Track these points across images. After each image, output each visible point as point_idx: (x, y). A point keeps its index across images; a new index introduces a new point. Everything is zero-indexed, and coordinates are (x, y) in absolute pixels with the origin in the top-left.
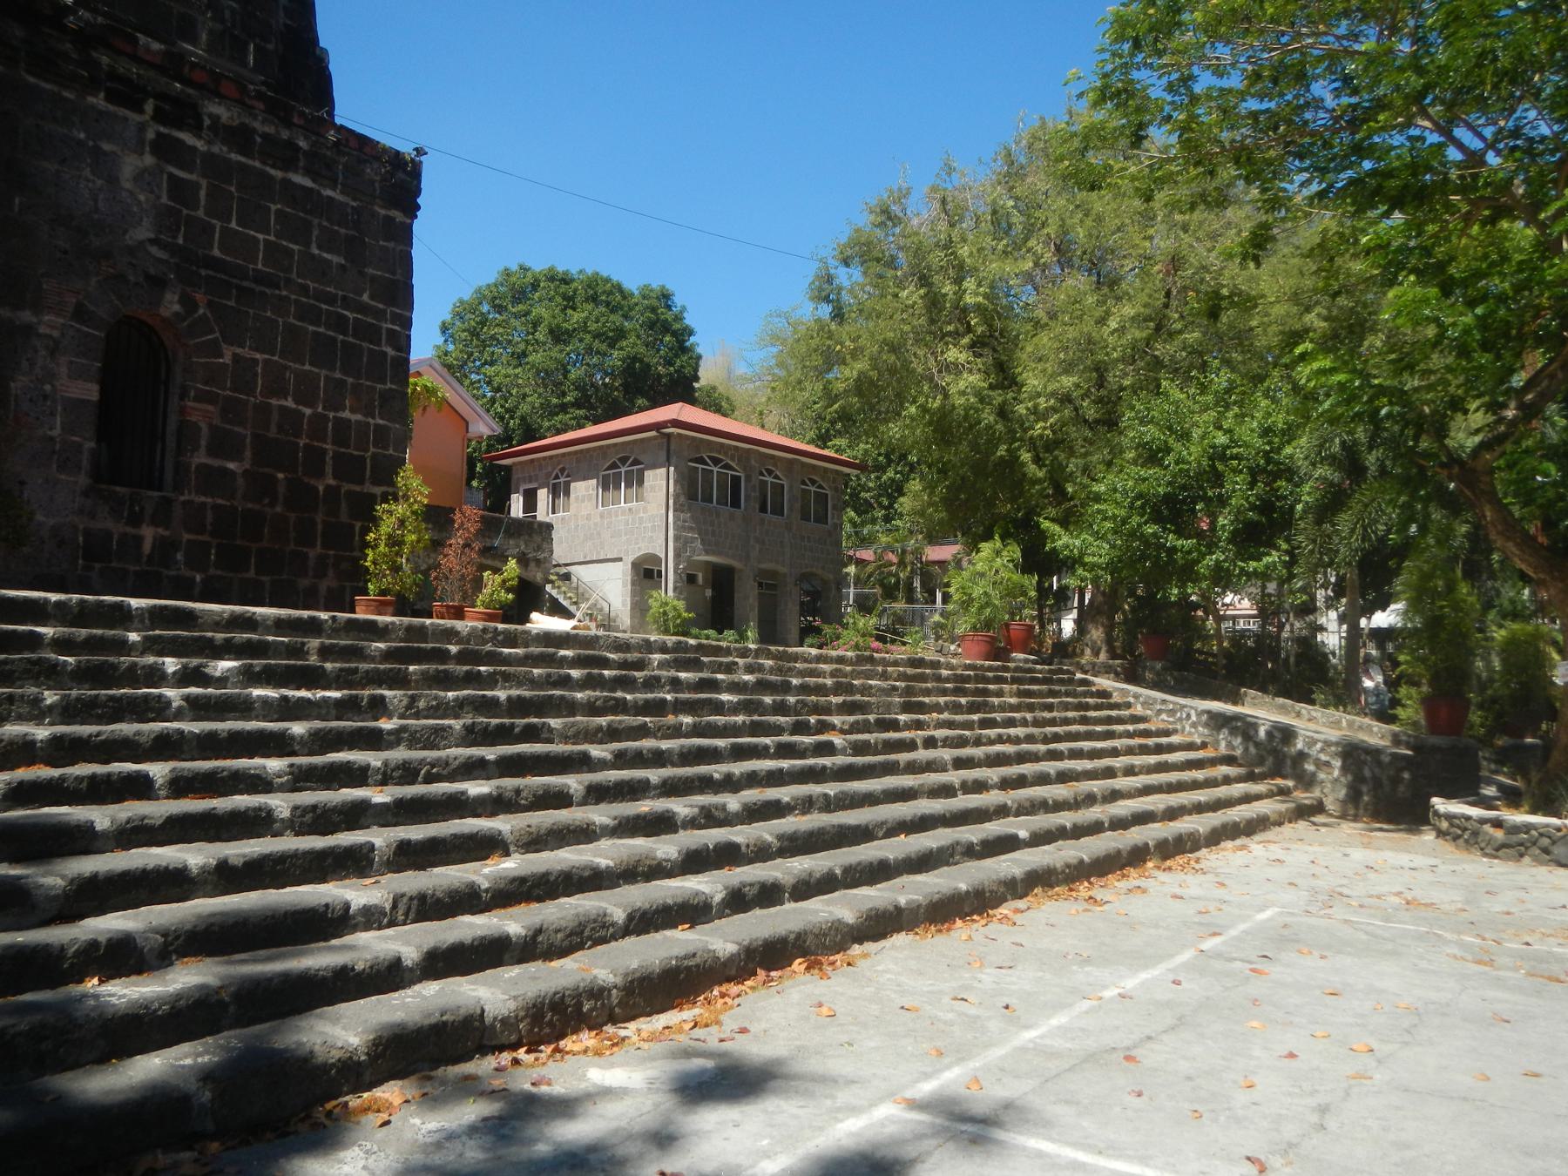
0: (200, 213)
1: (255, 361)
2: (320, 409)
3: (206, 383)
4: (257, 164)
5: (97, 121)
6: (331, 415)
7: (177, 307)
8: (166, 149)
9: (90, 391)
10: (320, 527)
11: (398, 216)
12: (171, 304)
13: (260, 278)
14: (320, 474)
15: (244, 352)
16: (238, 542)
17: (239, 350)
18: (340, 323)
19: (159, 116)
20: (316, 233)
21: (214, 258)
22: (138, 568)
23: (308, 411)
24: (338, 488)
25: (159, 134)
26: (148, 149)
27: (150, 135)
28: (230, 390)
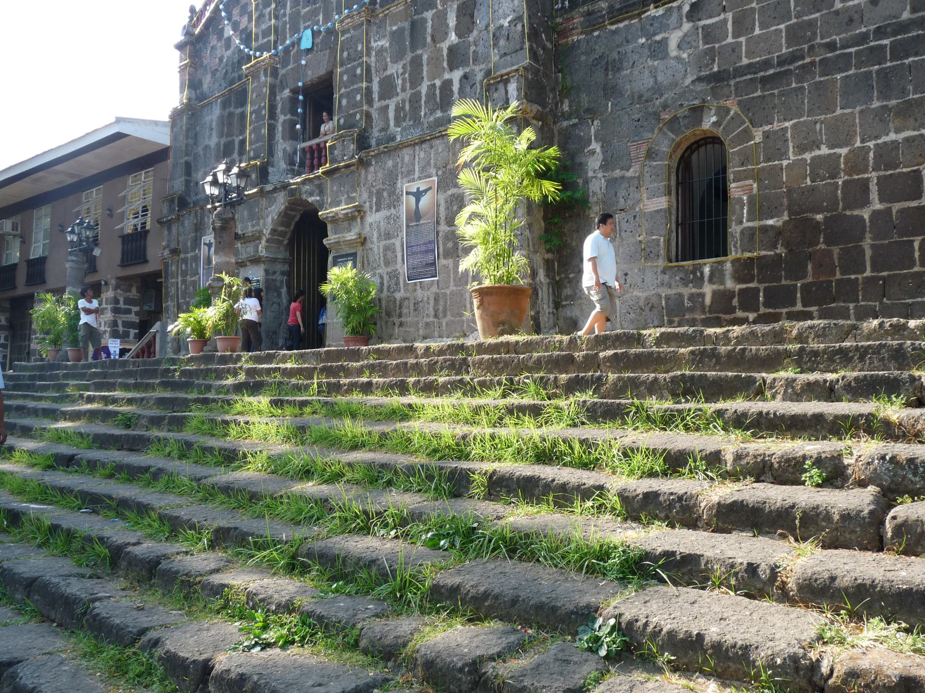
0: (730, 40)
1: (785, 130)
2: (858, 144)
3: (742, 165)
5: (651, 25)
6: (871, 144)
7: (714, 119)
9: (662, 202)
10: (868, 253)
12: (709, 121)
13: (782, 61)
14: (866, 202)
15: (776, 126)
16: (784, 282)
17: (767, 128)
18: (877, 54)
21: (750, 65)
22: (703, 317)
23: (844, 151)
24: (889, 210)
26: (685, 20)
28: (764, 162)
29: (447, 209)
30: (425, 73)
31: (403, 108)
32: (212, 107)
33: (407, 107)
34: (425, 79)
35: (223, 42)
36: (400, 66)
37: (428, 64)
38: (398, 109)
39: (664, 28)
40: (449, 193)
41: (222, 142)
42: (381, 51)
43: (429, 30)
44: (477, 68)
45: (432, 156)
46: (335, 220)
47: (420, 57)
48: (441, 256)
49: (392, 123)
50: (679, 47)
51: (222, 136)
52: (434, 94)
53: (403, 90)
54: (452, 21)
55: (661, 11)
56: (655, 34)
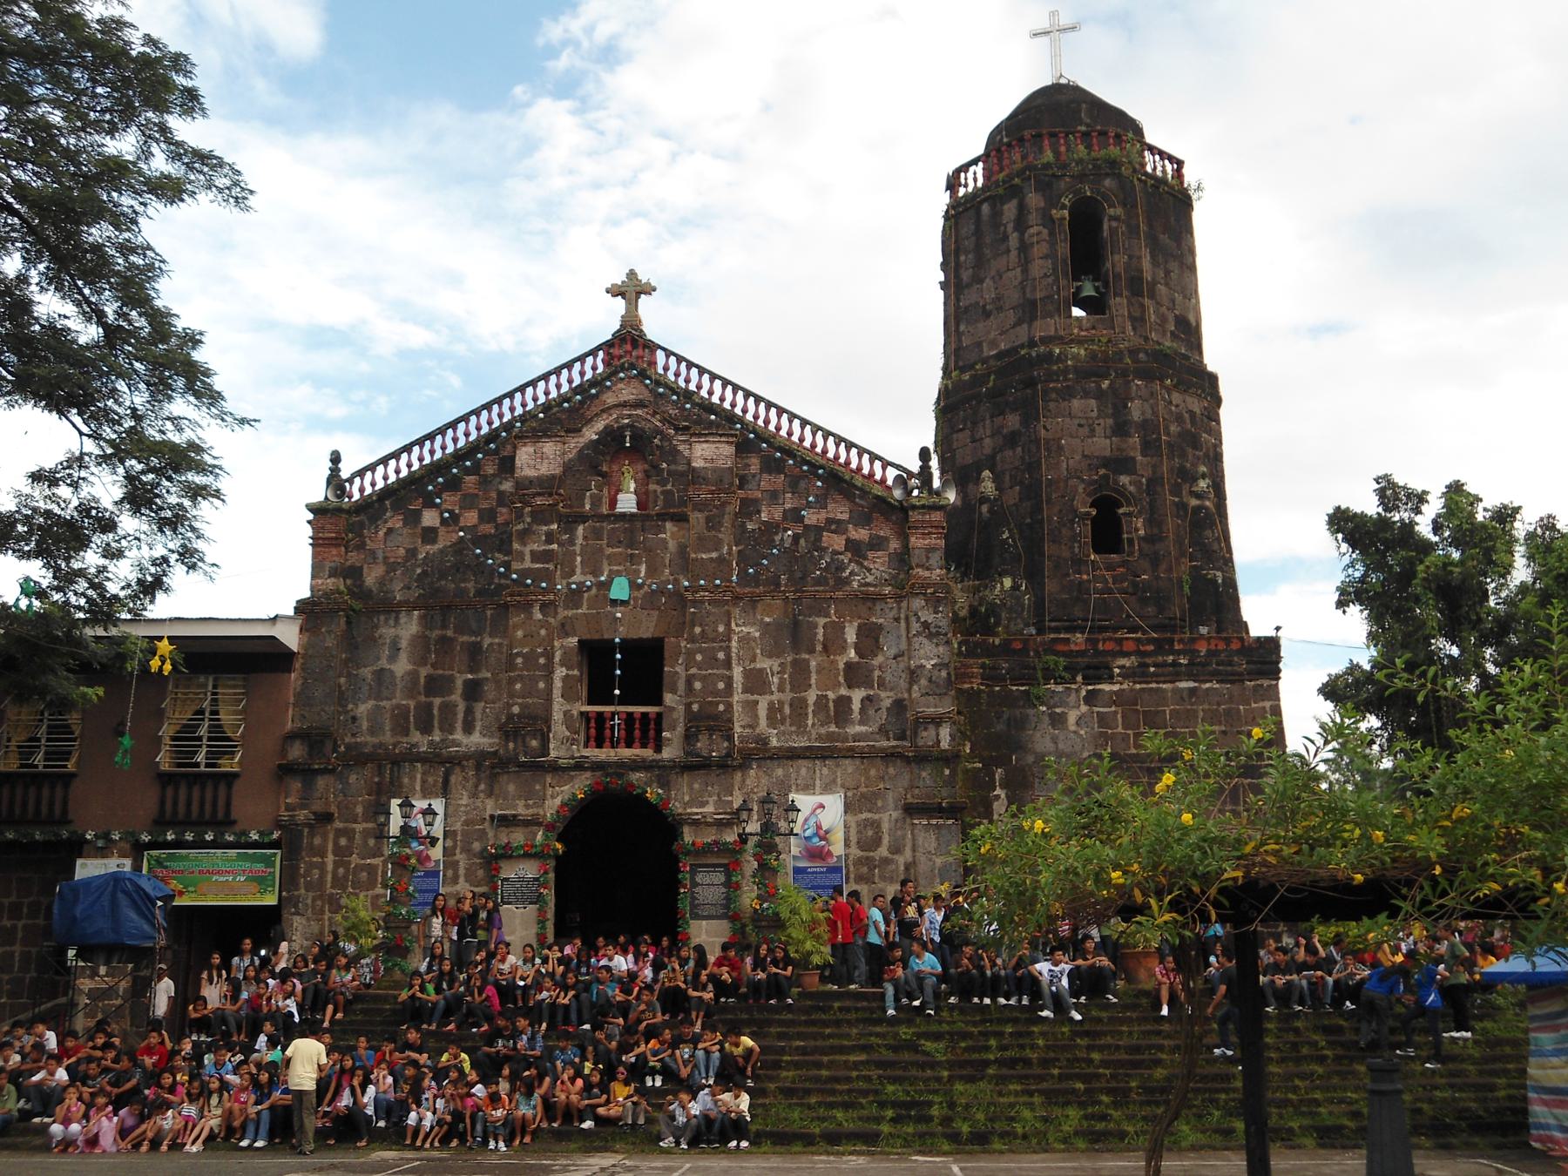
0: (1120, 729)
4: (1154, 685)
8: (1091, 698)
11: (1266, 683)
19: (1088, 680)
20: (1201, 714)
25: (1088, 691)
27: (1083, 693)
29: (859, 832)
30: (813, 681)
31: (781, 710)
32: (397, 619)
33: (787, 710)
34: (814, 686)
35: (419, 530)
36: (776, 664)
37: (818, 672)
38: (773, 710)
39: (1063, 704)
40: (864, 816)
41: (424, 672)
42: (745, 640)
43: (820, 637)
44: (883, 694)
45: (839, 774)
46: (696, 823)
47: (807, 662)
48: (852, 880)
49: (763, 722)
50: (1077, 724)
51: (422, 661)
52: (827, 706)
53: (781, 689)
54: (851, 635)
55: (1060, 688)
56: (1056, 706)
